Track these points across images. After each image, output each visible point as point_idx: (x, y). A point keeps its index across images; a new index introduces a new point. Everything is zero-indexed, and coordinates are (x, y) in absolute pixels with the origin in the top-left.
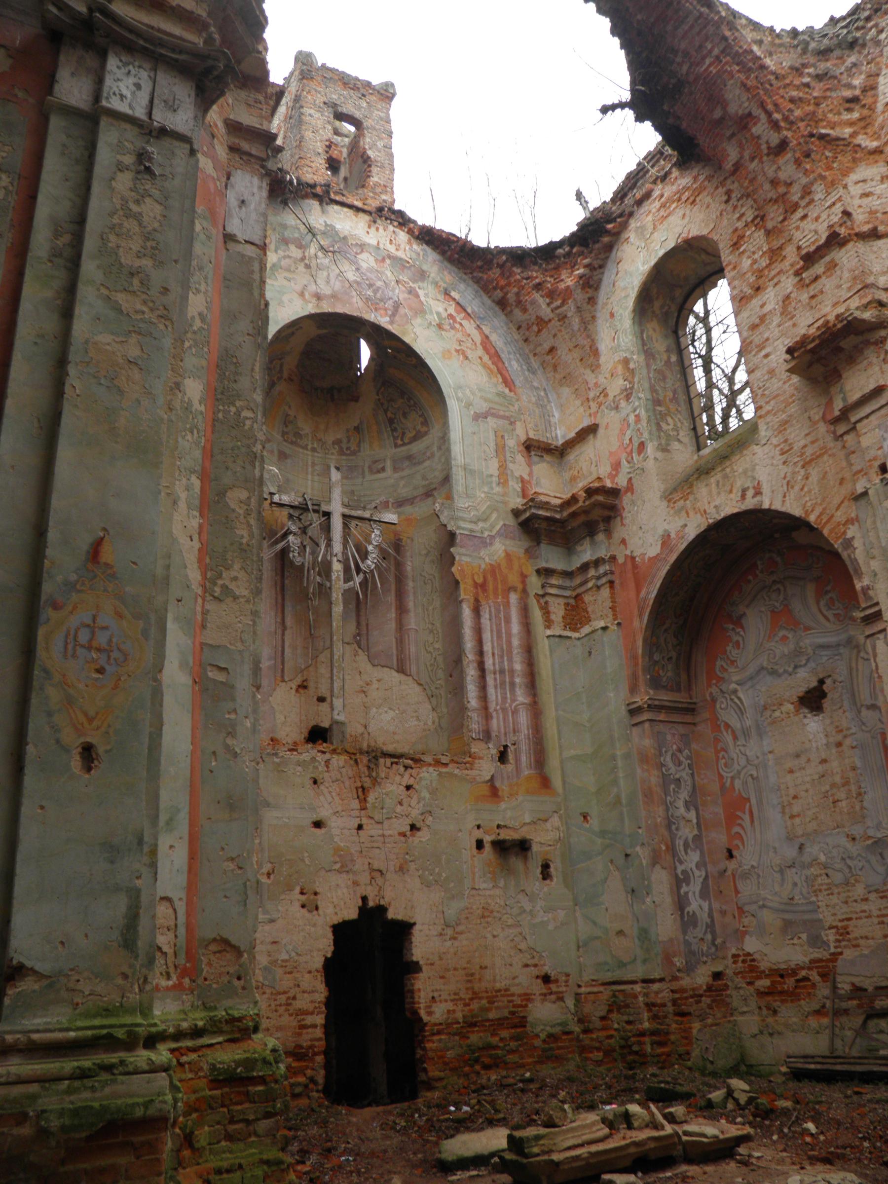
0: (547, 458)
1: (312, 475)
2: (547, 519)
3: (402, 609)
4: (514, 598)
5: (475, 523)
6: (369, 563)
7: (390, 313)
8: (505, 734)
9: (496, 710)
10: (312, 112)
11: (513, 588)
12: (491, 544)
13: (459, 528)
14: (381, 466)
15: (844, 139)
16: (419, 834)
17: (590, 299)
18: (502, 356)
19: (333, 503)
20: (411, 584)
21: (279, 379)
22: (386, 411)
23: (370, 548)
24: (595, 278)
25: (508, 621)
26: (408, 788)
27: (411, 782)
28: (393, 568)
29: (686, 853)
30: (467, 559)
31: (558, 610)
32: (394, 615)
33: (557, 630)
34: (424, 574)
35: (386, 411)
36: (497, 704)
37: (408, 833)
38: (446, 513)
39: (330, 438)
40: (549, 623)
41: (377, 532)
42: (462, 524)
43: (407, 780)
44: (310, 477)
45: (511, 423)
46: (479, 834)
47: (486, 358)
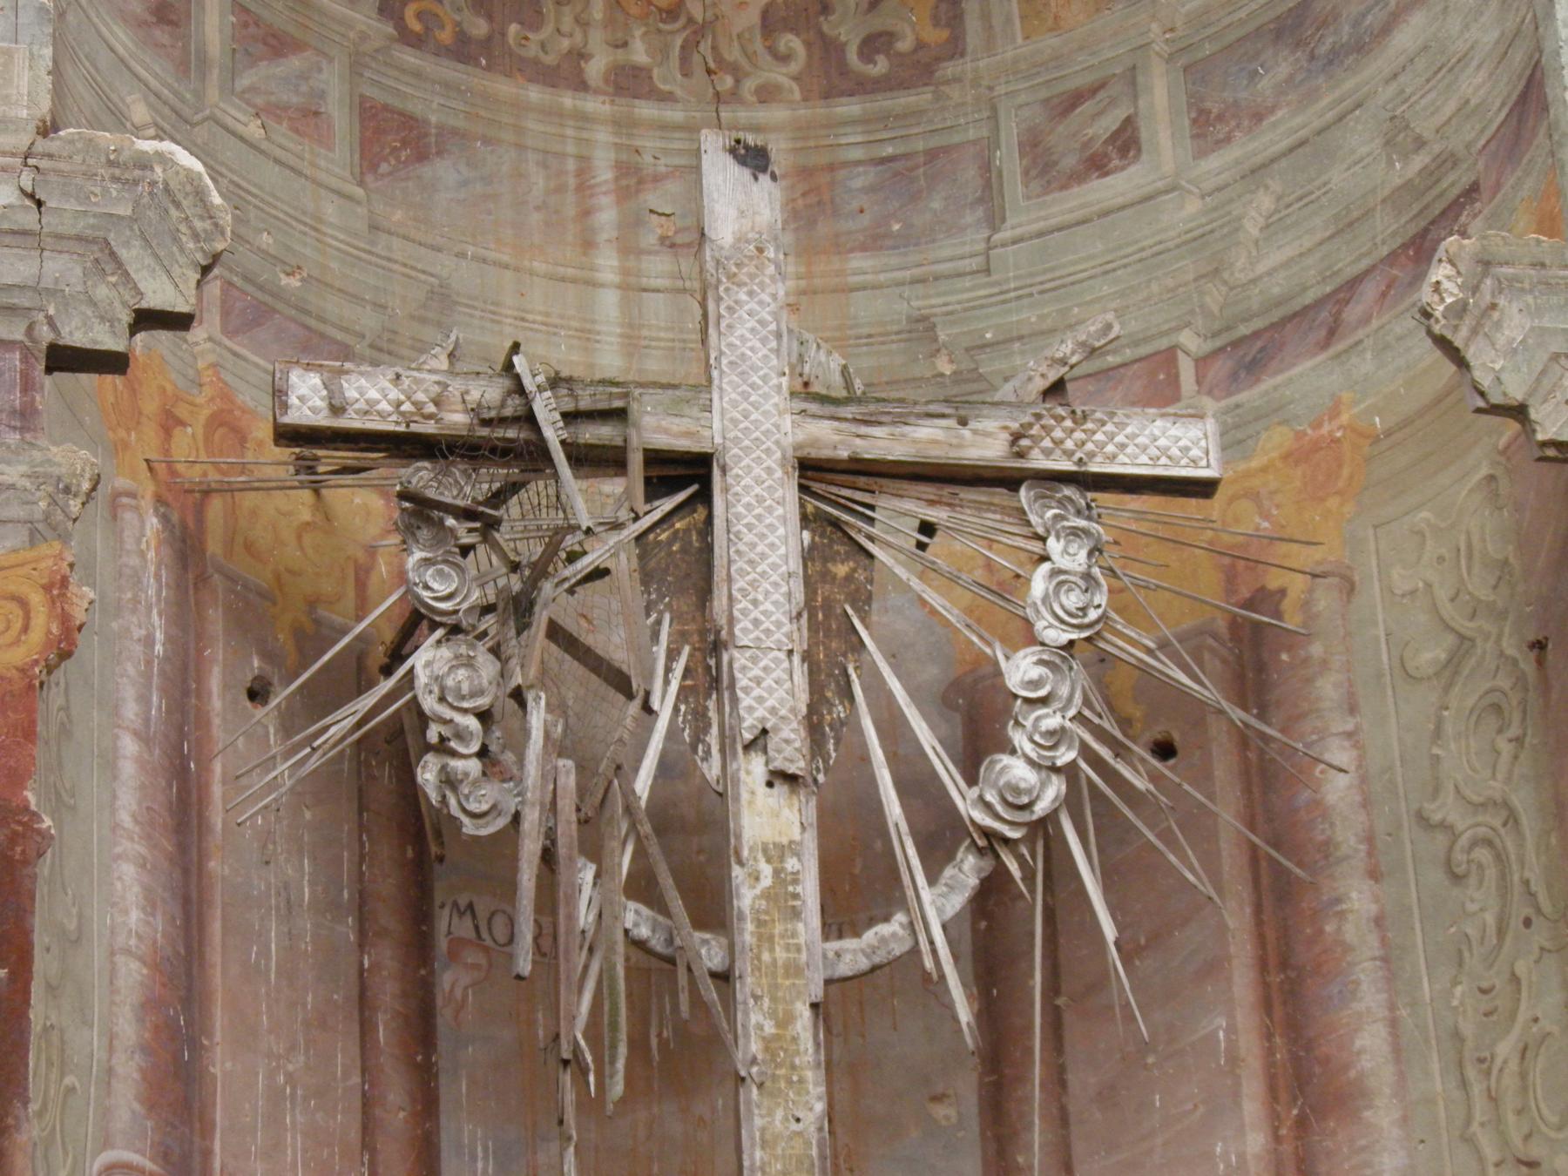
1: (628, 248)
6: (1017, 771)
14: (1110, 122)
19: (727, 392)
20: (1359, 899)
23: (1020, 670)
28: (1228, 814)
32: (1256, 1142)
34: (1446, 809)
38: (1514, 323)
41: (1069, 556)
44: (607, 263)
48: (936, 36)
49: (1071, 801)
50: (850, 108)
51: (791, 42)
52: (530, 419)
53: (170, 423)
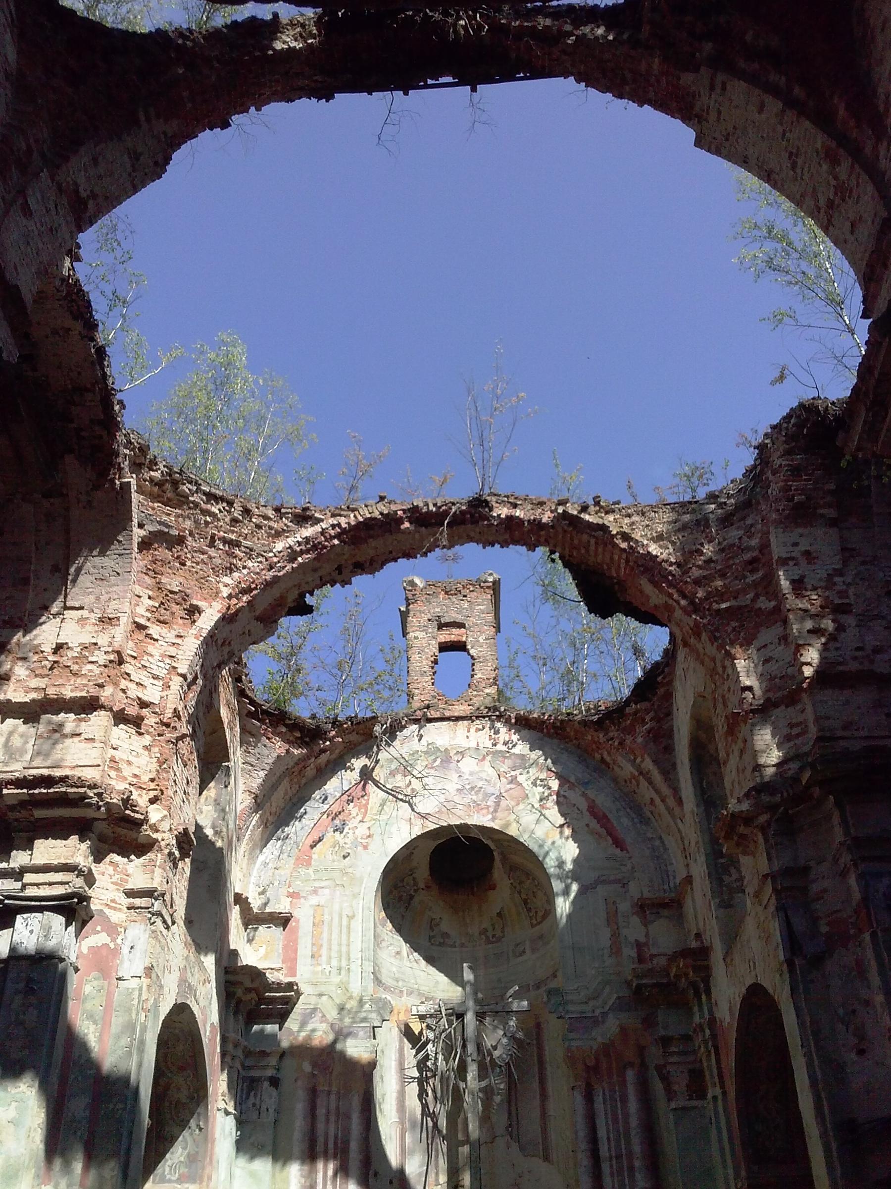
0: (665, 912)
3: (544, 1095)
4: (630, 1075)
7: (491, 809)
10: (417, 634)
11: (631, 1065)
12: (603, 1022)
13: (567, 1012)
15: (746, 606)
18: (610, 816)
21: (416, 891)
22: (519, 893)
25: (624, 1099)
30: (579, 1043)
31: (681, 1082)
33: (682, 1103)
40: (670, 1095)
42: (571, 1008)
45: (624, 886)
47: (594, 824)
48: (501, 935)
49: (511, 1059)
50: (490, 946)
51: (483, 937)
52: (440, 1011)
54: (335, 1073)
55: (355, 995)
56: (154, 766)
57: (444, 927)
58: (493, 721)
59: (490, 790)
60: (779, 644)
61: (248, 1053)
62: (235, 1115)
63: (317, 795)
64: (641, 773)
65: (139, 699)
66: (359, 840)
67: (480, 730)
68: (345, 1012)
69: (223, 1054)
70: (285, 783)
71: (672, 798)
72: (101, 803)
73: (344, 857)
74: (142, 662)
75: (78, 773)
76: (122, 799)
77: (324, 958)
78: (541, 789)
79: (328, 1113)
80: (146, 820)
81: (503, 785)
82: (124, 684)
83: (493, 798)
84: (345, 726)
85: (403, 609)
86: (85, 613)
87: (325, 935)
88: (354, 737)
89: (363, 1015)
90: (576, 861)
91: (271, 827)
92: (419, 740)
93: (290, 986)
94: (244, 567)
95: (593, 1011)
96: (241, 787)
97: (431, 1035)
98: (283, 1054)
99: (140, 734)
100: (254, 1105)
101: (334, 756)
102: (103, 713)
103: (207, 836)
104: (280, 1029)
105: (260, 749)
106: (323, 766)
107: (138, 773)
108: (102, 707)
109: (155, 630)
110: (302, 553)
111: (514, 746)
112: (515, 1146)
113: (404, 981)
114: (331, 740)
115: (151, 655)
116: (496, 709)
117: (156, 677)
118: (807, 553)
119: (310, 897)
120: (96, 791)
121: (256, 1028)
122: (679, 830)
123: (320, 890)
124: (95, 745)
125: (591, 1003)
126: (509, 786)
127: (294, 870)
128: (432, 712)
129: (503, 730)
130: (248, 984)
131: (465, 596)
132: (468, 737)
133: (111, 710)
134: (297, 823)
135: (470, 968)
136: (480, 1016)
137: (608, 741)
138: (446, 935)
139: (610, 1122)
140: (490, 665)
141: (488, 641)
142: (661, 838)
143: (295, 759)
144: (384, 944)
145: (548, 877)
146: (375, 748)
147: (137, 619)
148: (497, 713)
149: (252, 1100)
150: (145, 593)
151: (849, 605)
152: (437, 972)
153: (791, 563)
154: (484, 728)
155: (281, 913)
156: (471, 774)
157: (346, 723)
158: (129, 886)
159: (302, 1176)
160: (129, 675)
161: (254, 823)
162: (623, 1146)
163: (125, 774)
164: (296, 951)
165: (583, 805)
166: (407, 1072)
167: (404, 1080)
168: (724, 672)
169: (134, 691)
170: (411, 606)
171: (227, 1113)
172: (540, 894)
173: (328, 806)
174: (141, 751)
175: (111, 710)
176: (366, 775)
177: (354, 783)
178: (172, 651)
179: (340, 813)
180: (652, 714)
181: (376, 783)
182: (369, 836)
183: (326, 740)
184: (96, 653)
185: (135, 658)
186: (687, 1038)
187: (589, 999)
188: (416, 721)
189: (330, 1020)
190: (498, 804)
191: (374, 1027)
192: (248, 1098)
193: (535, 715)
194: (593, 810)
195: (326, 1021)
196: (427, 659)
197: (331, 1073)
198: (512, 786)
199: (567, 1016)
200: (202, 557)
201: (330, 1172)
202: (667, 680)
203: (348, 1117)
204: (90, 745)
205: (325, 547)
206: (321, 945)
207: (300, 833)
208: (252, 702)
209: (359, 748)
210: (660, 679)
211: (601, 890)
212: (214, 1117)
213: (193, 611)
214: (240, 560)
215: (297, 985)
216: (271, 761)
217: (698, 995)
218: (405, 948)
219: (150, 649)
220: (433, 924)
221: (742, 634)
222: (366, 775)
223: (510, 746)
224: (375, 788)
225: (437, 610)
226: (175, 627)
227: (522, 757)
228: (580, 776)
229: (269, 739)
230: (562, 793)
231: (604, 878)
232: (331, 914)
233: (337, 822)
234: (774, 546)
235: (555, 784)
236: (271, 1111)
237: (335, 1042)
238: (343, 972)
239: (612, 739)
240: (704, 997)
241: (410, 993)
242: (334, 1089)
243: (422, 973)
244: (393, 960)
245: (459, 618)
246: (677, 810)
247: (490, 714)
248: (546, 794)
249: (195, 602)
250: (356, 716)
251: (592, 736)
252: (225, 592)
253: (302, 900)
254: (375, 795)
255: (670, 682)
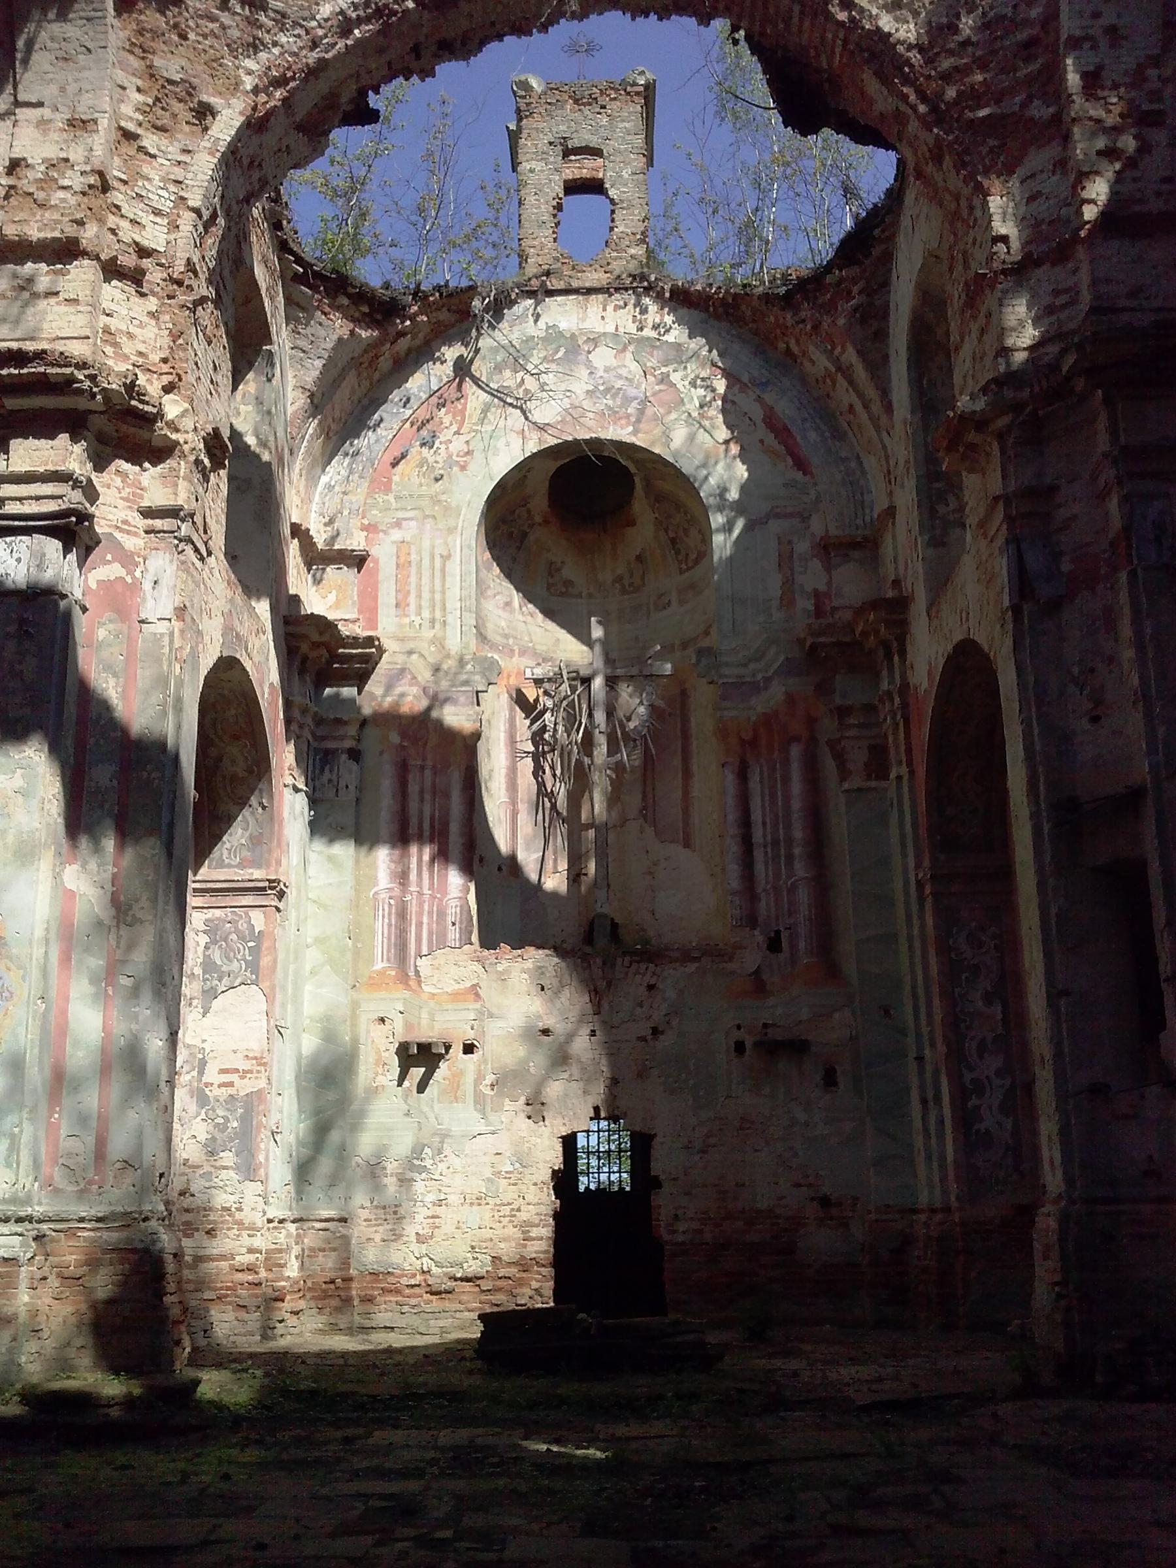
0: (856, 554)
2: (839, 644)
3: (687, 774)
4: (795, 751)
5: (745, 665)
7: (633, 419)
8: (777, 917)
9: (764, 890)
10: (533, 164)
11: (796, 739)
12: (766, 688)
13: (721, 676)
15: (1014, 113)
16: (662, 1037)
17: (876, 334)
18: (794, 430)
20: (695, 743)
21: (531, 526)
22: (666, 531)
24: (878, 303)
25: (786, 779)
26: (651, 987)
27: (652, 982)
29: (981, 1057)
30: (733, 713)
31: (858, 757)
33: (856, 782)
35: (666, 531)
36: (767, 883)
37: (649, 1037)
39: (606, 576)
40: (844, 774)
42: (726, 671)
43: (648, 979)
46: (738, 1035)
47: (770, 439)
53: (509, 676)
54: (430, 745)
55: (453, 653)
56: (166, 341)
57: (568, 572)
58: (638, 296)
59: (632, 392)
60: (1054, 173)
61: (319, 721)
62: (306, 792)
63: (396, 396)
64: (839, 369)
65: (137, 244)
66: (454, 458)
67: (621, 308)
68: (441, 674)
69: (288, 721)
70: (351, 378)
71: (878, 403)
72: (95, 390)
73: (437, 480)
74: (136, 189)
75: (60, 347)
76: (125, 384)
77: (413, 607)
78: (701, 392)
79: (422, 792)
80: (160, 415)
81: (649, 386)
82: (112, 221)
83: (635, 404)
84: (431, 299)
85: (513, 127)
86: (46, 112)
87: (413, 579)
88: (444, 315)
89: (464, 677)
90: (744, 488)
91: (334, 438)
92: (536, 321)
93: (370, 641)
94: (275, 44)
95: (754, 675)
96: (291, 381)
97: (549, 703)
98: (364, 723)
99: (143, 295)
100: (330, 781)
101: (418, 342)
102: (86, 262)
103: (249, 446)
104: (359, 693)
105: (313, 328)
106: (402, 354)
107: (144, 350)
108: (84, 254)
109: (150, 141)
110: (359, 21)
111: (667, 331)
112: (650, 831)
113: (515, 638)
114: (412, 318)
115: (148, 179)
116: (643, 277)
117: (157, 212)
118: (1112, 30)
119: (391, 531)
120: (86, 372)
121: (328, 691)
122: (884, 447)
123: (404, 523)
124: (80, 308)
125: (752, 666)
126: (657, 388)
127: (369, 495)
128: (554, 281)
129: (653, 308)
130: (315, 637)
131: (603, 107)
132: (603, 318)
133: (97, 258)
134: (370, 433)
135: (599, 622)
136: (611, 682)
137: (798, 323)
138: (568, 583)
139: (767, 804)
140: (638, 213)
141: (636, 177)
142: (858, 457)
143: (364, 345)
144: (489, 593)
145: (705, 509)
146: (474, 333)
147: (123, 124)
148: (646, 284)
149: (327, 775)
150: (132, 82)
151: (1160, 113)
152: (558, 628)
153: (1087, 45)
154: (626, 305)
155: (354, 551)
156: (607, 369)
157: (432, 295)
158: (146, 503)
159: (392, 861)
160: (118, 207)
161: (311, 431)
162: (781, 831)
163: (126, 351)
164: (376, 599)
165: (758, 413)
166: (519, 746)
167: (515, 754)
168: (970, 214)
169: (128, 233)
170: (524, 122)
171: (296, 790)
172: (693, 532)
173: (411, 412)
174: (146, 319)
175: (97, 258)
176: (461, 369)
177: (445, 380)
178: (178, 173)
179: (428, 421)
180: (861, 284)
181: (476, 381)
182: (468, 453)
183: (404, 318)
184: (69, 173)
185: (125, 182)
186: (871, 708)
187: (750, 661)
188: (531, 294)
189: (423, 683)
190: (641, 412)
191: (477, 692)
192: (322, 771)
193: (699, 287)
194: (771, 422)
195: (417, 684)
196: (547, 203)
197: (425, 744)
198: (662, 387)
199: (721, 681)
200: (211, 25)
201: (426, 857)
202: (887, 234)
203: (447, 795)
204: (71, 309)
205: (395, 13)
206: (409, 592)
207: (376, 448)
208: (299, 260)
209: (451, 331)
210: (876, 232)
211: (775, 526)
212: (281, 794)
213: (204, 113)
214: (268, 32)
215: (378, 639)
216: (330, 345)
217: (889, 656)
218: (516, 598)
219: (146, 170)
220: (552, 570)
221: (1002, 158)
222: (462, 369)
223: (662, 331)
224: (475, 387)
225: (561, 128)
226: (179, 136)
227: (678, 346)
228: (756, 373)
229: (325, 314)
230: (730, 397)
231: (778, 510)
232: (419, 552)
233: (424, 433)
234: (1064, 16)
235: (721, 385)
236: (352, 788)
237: (429, 709)
238: (437, 626)
239: (803, 321)
240: (896, 658)
241: (523, 653)
242: (429, 763)
243: (538, 629)
244: (500, 612)
245: (594, 141)
246: (884, 420)
247: (635, 285)
248: (708, 399)
249: (205, 98)
250: (446, 285)
251: (776, 317)
252: (248, 83)
253: (381, 534)
254: (475, 398)
255: (891, 238)
